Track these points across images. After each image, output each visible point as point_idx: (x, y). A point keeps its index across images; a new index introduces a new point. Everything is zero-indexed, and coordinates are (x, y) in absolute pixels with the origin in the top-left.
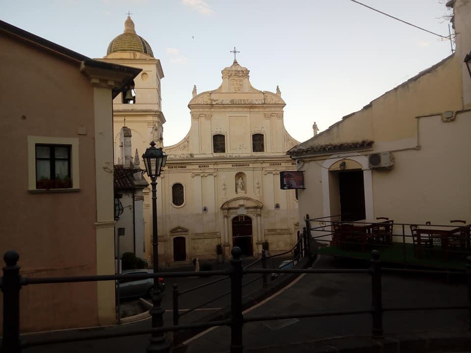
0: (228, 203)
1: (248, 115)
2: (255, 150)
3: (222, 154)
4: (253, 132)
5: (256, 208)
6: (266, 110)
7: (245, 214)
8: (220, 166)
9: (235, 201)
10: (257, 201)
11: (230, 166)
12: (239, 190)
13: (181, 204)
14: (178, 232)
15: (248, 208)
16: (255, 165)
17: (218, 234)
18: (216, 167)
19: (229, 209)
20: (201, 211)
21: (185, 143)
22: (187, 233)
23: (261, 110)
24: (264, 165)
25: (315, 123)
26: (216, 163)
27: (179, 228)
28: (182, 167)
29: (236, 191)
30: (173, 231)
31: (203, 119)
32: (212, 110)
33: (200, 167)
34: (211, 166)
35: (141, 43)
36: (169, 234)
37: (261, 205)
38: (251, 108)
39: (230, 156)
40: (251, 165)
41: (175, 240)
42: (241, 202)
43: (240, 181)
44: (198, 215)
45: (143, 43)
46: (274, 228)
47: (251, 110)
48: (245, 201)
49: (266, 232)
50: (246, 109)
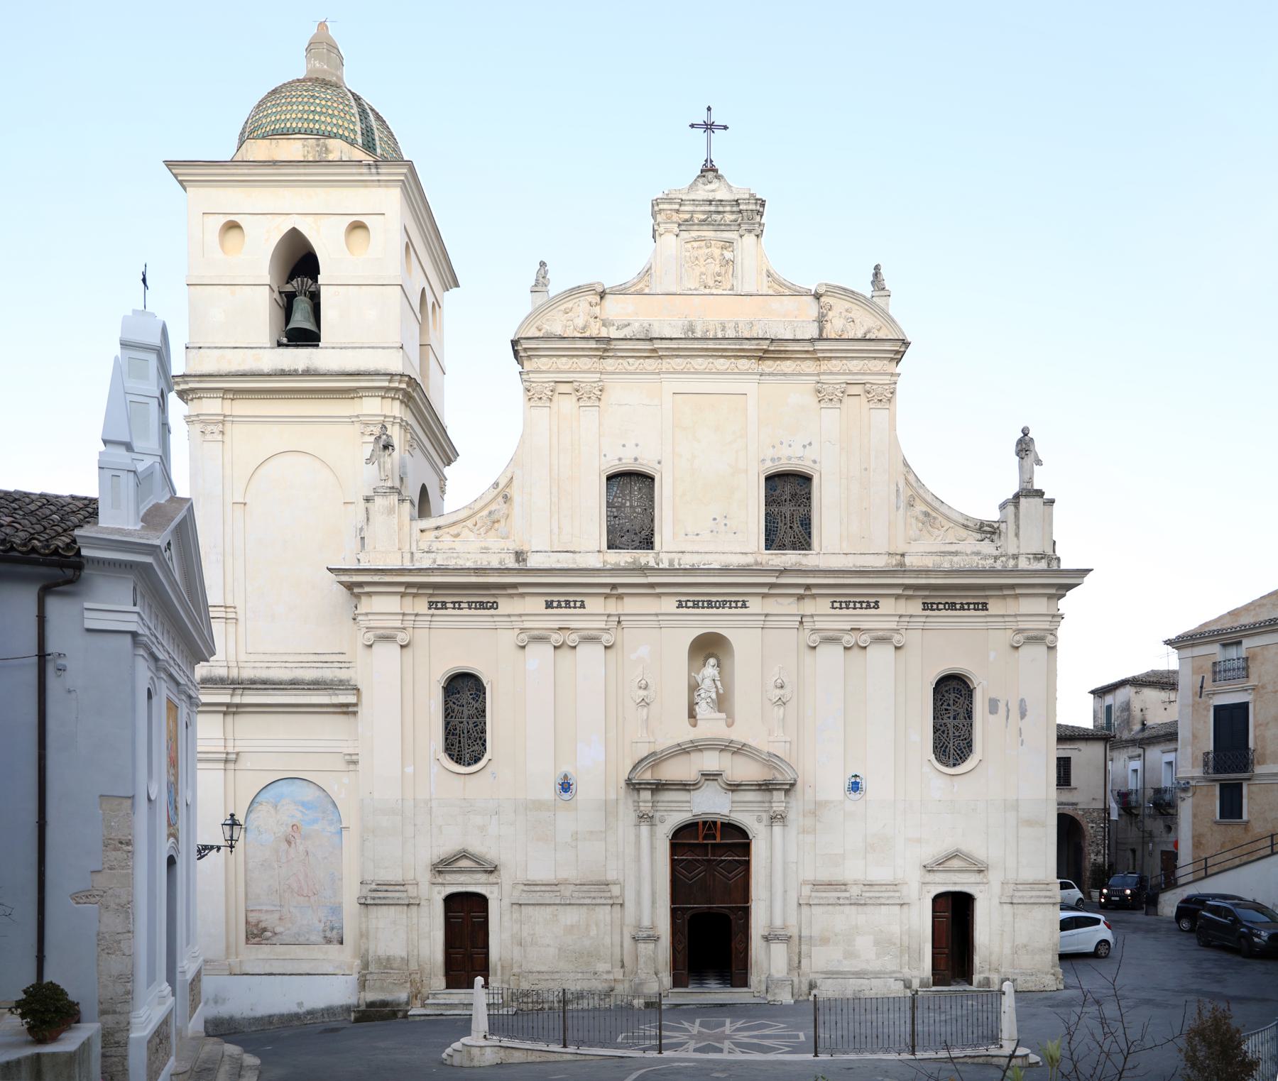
0: (655, 760)
1: (750, 386)
2: (773, 540)
3: (645, 557)
4: (769, 464)
5: (766, 787)
6: (825, 366)
7: (726, 812)
8: (631, 605)
9: (684, 758)
10: (771, 760)
11: (669, 605)
12: (703, 710)
13: (477, 760)
14: (461, 871)
15: (734, 787)
16: (772, 606)
17: (616, 890)
18: (612, 607)
19: (659, 787)
20: (548, 791)
21: (493, 507)
22: (492, 878)
23: (809, 366)
24: (809, 607)
25: (1025, 432)
26: (614, 591)
27: (464, 855)
28: (482, 606)
29: (692, 715)
30: (443, 867)
31: (566, 404)
32: (610, 364)
33: (549, 605)
34: (594, 605)
35: (355, 110)
36: (425, 876)
37: (788, 777)
38: (763, 356)
39: (671, 562)
40: (755, 605)
41: (451, 901)
42: (711, 761)
43: (710, 670)
44: (538, 805)
45: (363, 113)
46: (837, 876)
47: (768, 366)
48: (727, 757)
49: (806, 890)
50: (744, 364)
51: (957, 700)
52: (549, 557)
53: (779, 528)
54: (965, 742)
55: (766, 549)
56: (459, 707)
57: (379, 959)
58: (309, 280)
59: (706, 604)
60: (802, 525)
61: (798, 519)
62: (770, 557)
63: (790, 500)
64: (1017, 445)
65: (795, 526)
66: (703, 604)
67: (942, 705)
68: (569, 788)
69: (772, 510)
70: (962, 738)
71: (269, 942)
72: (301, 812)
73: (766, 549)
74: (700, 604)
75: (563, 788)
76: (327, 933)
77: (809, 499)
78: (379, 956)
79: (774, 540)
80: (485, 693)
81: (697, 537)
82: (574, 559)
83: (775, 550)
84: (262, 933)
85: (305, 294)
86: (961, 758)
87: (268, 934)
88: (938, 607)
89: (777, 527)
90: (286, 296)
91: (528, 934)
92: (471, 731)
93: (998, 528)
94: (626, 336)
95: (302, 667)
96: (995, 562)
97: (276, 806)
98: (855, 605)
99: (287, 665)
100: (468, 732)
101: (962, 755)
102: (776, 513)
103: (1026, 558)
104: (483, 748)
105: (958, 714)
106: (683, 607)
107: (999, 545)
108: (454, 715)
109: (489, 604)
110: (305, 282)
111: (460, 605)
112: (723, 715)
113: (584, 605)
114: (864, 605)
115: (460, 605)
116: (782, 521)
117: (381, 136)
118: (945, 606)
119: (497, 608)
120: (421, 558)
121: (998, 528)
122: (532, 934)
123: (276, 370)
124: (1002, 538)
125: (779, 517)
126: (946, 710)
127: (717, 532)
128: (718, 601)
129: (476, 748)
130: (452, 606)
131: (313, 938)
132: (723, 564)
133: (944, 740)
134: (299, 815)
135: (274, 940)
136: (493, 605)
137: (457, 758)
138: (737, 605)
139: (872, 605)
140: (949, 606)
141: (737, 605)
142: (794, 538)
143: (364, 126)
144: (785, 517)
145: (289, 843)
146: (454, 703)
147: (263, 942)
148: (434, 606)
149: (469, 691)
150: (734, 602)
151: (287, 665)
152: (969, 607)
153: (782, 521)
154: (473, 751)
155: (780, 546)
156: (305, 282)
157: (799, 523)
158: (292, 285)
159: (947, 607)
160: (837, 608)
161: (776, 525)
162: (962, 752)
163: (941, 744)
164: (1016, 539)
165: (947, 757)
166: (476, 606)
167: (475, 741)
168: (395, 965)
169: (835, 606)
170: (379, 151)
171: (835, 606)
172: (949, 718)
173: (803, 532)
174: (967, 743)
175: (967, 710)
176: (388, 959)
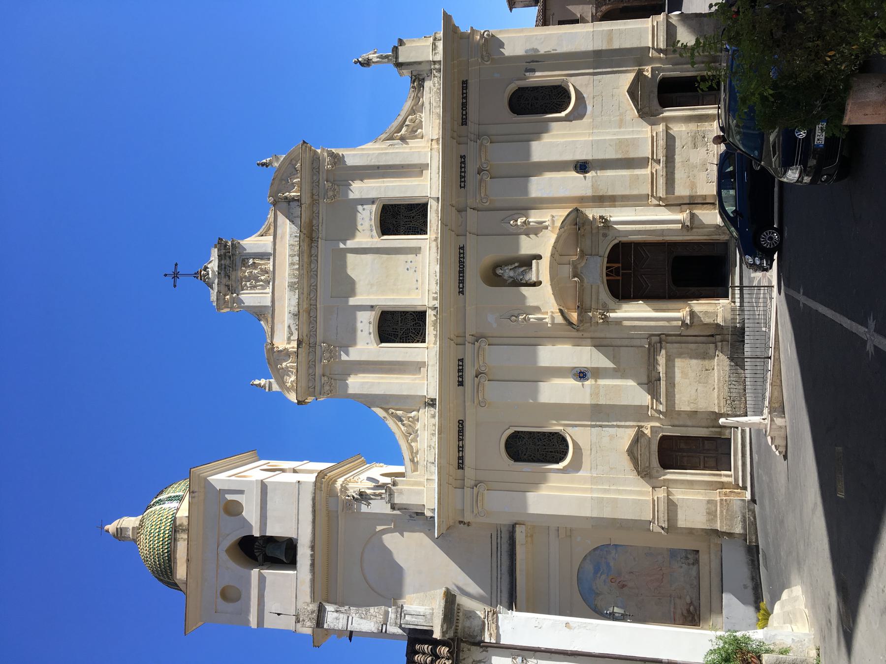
2: (420, 228)
3: (430, 317)
4: (374, 233)
51: (525, 99)
52: (430, 383)
53: (413, 226)
54: (553, 91)
55: (427, 234)
56: (528, 451)
57: (709, 520)
58: (256, 544)
59: (461, 275)
60: (411, 210)
61: (408, 213)
62: (432, 231)
63: (396, 218)
64: (365, 66)
65: (413, 215)
66: (461, 277)
67: (529, 109)
68: (583, 373)
69: (402, 230)
70: (550, 93)
71: (698, 608)
72: (601, 575)
73: (427, 234)
74: (461, 278)
75: (583, 377)
76: (690, 562)
77: (395, 205)
78: (707, 520)
79: (421, 229)
80: (518, 432)
81: (415, 281)
82: (432, 366)
83: (427, 228)
84: (692, 613)
85: (265, 547)
86: (564, 93)
87: (692, 608)
88: (464, 115)
89: (413, 227)
90: (264, 562)
91: (688, 406)
92: (544, 443)
93: (415, 76)
94: (296, 329)
95: (501, 566)
96: (437, 77)
97: (598, 593)
98: (463, 172)
99: (499, 577)
100: (544, 445)
101: (562, 93)
102: (403, 228)
103: (434, 55)
104: (555, 435)
105: (534, 97)
106: (463, 291)
107: (426, 75)
108: (533, 455)
109: (460, 426)
110: (257, 547)
111: (461, 447)
112: (534, 262)
113: (461, 359)
114: (463, 165)
115: (461, 447)
116: (408, 224)
117: (172, 491)
118: (464, 110)
119: (462, 421)
120: (430, 473)
121: (415, 76)
122: (688, 403)
123: (310, 570)
124: (422, 73)
125: (406, 226)
126: (532, 106)
127: (416, 268)
128: (459, 266)
129: (555, 440)
130: (461, 453)
131: (694, 573)
132: (436, 263)
133: (552, 106)
134: (603, 577)
135: (696, 604)
136: (461, 423)
137: (563, 454)
138: (462, 253)
139: (463, 160)
140: (464, 107)
141: (462, 253)
142: (419, 215)
143: (167, 502)
144: (407, 222)
145: (624, 586)
146: (525, 455)
147: (698, 613)
148: (461, 465)
149: (517, 443)
150: (460, 255)
151: (499, 577)
152: (465, 93)
153: (409, 224)
154: (558, 442)
155: (425, 225)
156: (257, 547)
157: (410, 212)
158: (258, 556)
159: (465, 108)
160: (464, 185)
161: (411, 228)
162: (560, 92)
163: (555, 108)
164: (422, 64)
165: (563, 103)
166: (461, 436)
167: (551, 441)
168: (714, 509)
169: (463, 186)
170: (181, 493)
171: (463, 186)
172: (537, 103)
173: (416, 209)
174: (554, 89)
175: (532, 91)
176: (708, 513)
